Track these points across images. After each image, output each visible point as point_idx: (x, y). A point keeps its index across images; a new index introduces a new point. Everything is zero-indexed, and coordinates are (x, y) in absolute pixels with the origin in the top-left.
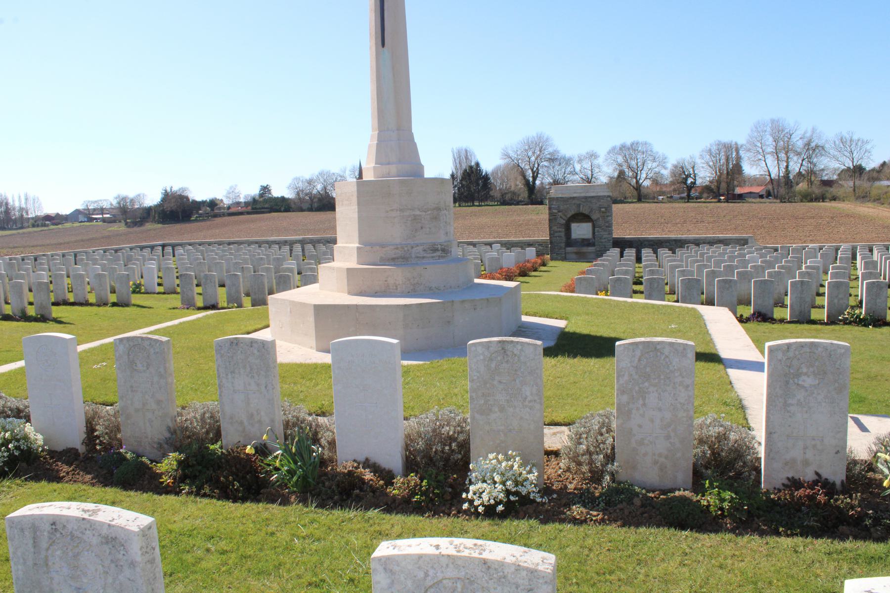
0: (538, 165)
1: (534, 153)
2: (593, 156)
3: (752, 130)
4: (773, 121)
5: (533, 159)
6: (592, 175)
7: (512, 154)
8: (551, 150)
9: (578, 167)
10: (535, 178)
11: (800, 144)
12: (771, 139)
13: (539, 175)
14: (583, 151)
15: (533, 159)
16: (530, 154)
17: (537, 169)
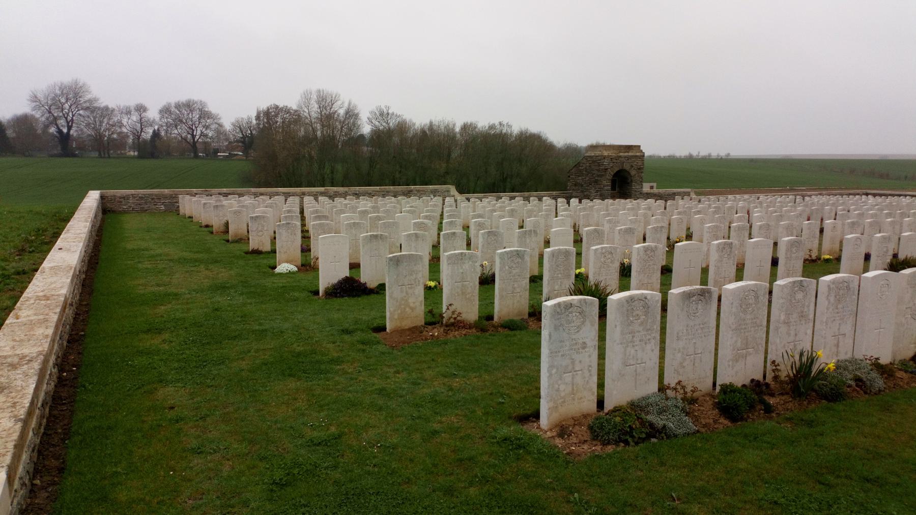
0: (73, 116)
1: (67, 100)
2: (141, 109)
3: (301, 97)
4: (319, 91)
5: (67, 106)
6: (142, 129)
7: (41, 96)
8: (88, 97)
9: (125, 121)
10: (69, 128)
11: (342, 112)
12: (316, 106)
13: (74, 125)
14: (132, 103)
15: (67, 106)
16: (63, 100)
17: (72, 118)
